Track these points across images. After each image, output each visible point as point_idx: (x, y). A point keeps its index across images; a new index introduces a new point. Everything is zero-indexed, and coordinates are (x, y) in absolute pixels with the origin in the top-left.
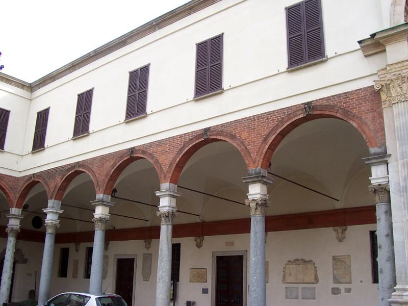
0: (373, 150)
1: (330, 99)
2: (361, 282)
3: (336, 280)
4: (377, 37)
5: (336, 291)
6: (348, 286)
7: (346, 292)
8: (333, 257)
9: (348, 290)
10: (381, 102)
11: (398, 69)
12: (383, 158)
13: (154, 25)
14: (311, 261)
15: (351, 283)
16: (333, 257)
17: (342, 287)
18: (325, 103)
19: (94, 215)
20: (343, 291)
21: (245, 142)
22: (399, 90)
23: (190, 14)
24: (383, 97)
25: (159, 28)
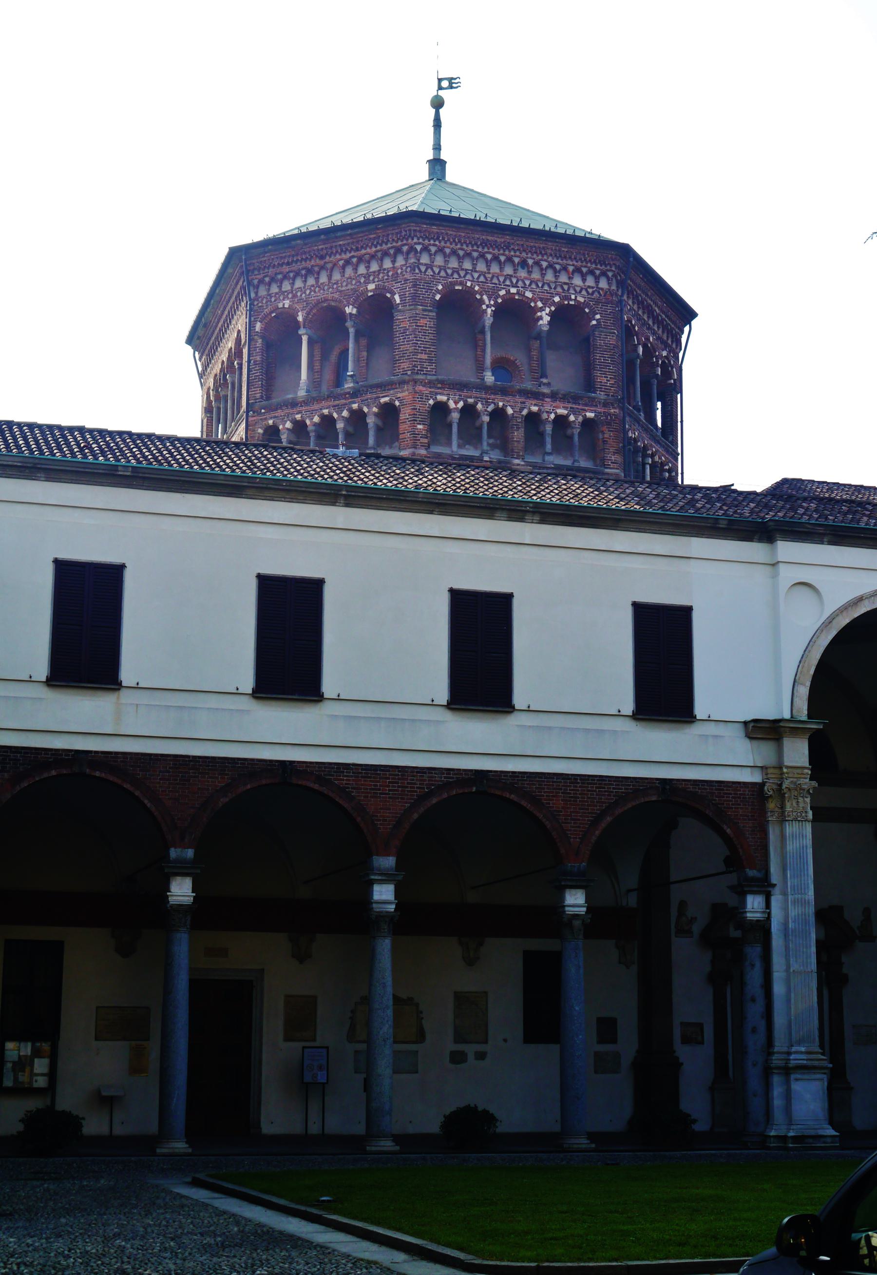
0: (751, 873)
1: (699, 785)
2: (505, 1040)
3: (459, 1038)
4: (781, 724)
5: (458, 1058)
6: (481, 1048)
7: (476, 1059)
8: (455, 992)
9: (481, 1056)
10: (766, 813)
11: (796, 776)
12: (765, 887)
13: (342, 495)
14: (411, 999)
15: (486, 1042)
16: (455, 992)
17: (470, 1049)
18: (691, 788)
19: (167, 897)
20: (471, 1056)
21: (560, 815)
22: (794, 804)
23: (431, 512)
24: (771, 805)
25: (347, 505)
